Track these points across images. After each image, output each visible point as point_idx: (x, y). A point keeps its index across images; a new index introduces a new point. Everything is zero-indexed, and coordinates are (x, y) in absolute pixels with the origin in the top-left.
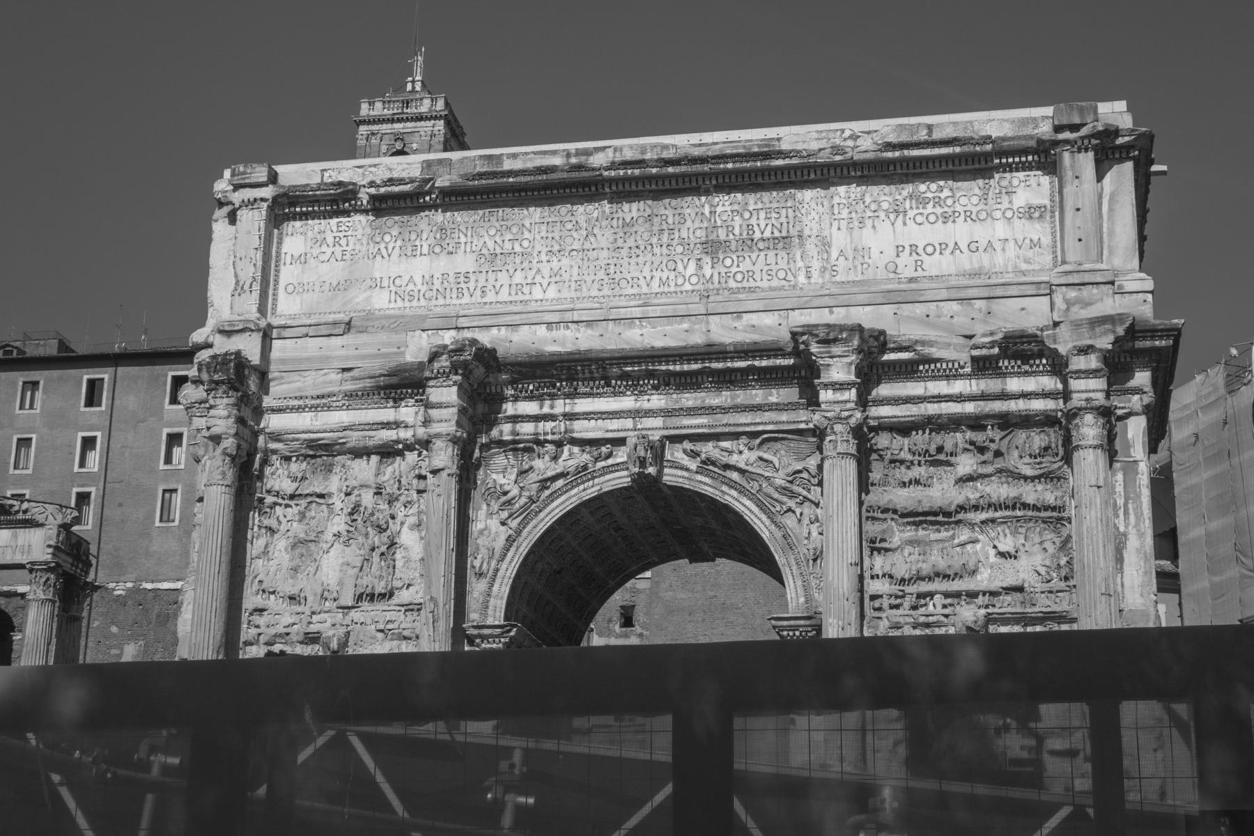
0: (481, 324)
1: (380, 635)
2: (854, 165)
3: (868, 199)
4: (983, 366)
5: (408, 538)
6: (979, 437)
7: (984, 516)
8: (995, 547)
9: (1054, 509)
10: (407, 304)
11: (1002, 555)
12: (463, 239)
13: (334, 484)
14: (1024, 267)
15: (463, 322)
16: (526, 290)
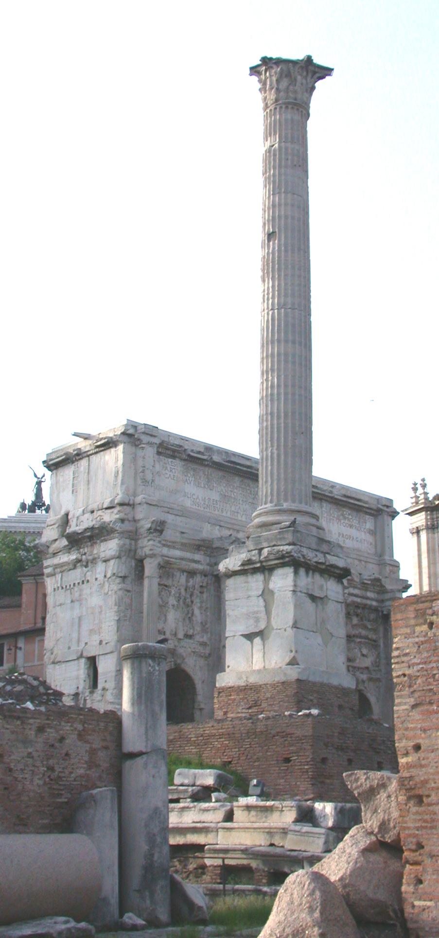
0: (228, 526)
1: (192, 654)
2: (332, 498)
3: (331, 512)
4: (364, 586)
5: (197, 612)
6: (359, 611)
7: (359, 640)
8: (361, 652)
9: (375, 641)
10: (197, 507)
11: (363, 655)
12: (215, 485)
13: (169, 582)
14: (369, 551)
15: (222, 523)
16: (236, 514)
